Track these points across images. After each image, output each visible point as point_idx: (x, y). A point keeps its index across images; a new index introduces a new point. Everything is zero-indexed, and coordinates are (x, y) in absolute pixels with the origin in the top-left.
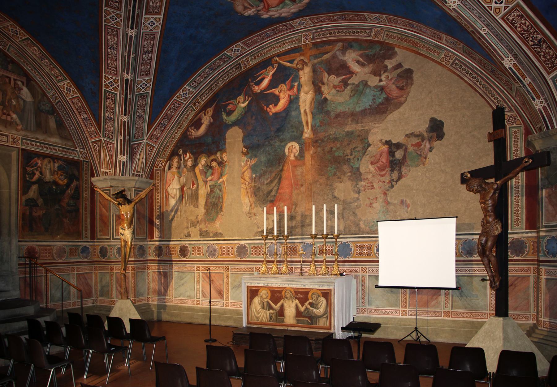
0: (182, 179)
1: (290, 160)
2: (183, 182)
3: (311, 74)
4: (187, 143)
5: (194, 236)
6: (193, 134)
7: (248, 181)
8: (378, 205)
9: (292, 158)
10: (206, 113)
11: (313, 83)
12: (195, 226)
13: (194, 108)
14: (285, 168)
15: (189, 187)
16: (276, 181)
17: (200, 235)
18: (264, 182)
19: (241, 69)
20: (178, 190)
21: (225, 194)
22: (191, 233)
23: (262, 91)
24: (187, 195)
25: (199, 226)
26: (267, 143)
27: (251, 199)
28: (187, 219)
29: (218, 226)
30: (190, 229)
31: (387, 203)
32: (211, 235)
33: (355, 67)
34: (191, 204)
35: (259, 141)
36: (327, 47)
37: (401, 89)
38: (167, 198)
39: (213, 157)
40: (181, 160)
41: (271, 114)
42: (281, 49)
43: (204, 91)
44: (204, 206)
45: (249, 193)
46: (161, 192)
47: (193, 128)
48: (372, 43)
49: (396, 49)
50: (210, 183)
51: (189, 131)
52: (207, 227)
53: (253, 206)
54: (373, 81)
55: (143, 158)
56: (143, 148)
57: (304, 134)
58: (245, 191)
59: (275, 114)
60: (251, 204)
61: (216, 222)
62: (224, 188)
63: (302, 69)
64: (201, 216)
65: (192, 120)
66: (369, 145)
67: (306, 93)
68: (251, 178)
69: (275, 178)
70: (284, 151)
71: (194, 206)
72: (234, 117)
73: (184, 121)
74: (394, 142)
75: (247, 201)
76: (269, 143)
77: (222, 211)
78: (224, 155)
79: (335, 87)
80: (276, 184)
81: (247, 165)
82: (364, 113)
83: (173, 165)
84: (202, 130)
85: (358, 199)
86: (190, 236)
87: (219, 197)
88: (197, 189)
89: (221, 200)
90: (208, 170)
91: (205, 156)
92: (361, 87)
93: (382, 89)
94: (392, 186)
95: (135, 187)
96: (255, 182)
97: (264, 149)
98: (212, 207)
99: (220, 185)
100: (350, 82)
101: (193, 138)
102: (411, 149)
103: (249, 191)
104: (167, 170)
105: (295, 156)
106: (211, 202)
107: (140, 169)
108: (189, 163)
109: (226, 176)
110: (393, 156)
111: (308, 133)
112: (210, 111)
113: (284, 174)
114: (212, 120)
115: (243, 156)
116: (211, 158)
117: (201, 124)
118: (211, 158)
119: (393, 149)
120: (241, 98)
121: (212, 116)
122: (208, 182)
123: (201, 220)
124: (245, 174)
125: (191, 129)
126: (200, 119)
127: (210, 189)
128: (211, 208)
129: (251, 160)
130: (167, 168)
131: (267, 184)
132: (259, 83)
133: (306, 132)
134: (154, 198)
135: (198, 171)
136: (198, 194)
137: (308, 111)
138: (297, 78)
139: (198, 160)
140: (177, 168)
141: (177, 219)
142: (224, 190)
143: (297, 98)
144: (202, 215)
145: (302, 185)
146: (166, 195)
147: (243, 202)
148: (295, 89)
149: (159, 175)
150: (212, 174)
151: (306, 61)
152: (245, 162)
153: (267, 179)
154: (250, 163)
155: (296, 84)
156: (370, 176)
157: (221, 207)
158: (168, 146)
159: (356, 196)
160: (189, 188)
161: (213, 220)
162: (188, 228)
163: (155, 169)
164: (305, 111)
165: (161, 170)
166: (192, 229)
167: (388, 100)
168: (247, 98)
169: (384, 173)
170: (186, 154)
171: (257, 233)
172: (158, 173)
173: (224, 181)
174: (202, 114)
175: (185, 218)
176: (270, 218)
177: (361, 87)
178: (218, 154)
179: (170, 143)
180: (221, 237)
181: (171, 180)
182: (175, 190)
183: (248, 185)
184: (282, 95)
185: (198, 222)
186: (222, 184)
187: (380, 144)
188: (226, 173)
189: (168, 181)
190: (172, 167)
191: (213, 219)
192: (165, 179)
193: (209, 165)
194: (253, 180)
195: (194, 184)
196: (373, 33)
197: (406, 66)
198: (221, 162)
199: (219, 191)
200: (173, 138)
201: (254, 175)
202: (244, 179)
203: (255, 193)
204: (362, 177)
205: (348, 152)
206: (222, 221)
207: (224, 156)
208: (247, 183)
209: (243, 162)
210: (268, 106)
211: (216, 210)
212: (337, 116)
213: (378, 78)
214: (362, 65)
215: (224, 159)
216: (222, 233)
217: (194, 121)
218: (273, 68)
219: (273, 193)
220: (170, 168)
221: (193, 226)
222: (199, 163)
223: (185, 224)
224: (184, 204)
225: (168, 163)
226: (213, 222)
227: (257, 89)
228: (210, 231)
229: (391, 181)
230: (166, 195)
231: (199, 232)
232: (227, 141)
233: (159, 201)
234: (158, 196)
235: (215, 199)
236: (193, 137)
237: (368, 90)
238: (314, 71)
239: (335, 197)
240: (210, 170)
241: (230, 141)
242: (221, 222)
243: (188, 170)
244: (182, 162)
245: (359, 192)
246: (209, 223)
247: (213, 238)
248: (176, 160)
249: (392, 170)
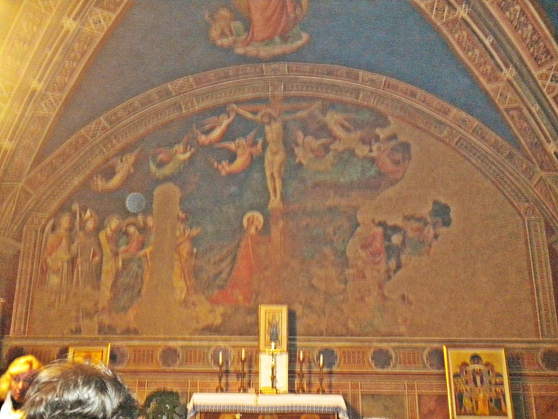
3: (281, 131)
8: (372, 300)
9: (253, 230)
10: (124, 159)
11: (285, 143)
14: (243, 244)
16: (229, 259)
18: (209, 259)
19: (182, 110)
23: (211, 144)
26: (217, 209)
31: (384, 298)
33: (339, 132)
36: (304, 104)
37: (397, 163)
39: (131, 219)
41: (223, 173)
42: (241, 96)
48: (359, 108)
49: (390, 118)
54: (362, 150)
57: (271, 202)
59: (231, 175)
63: (269, 123)
66: (358, 225)
67: (274, 153)
68: (191, 253)
70: (241, 222)
72: (167, 170)
74: (390, 223)
75: (182, 284)
79: (312, 151)
82: (351, 186)
84: (116, 181)
85: (344, 290)
89: (139, 280)
92: (346, 156)
93: (373, 161)
94: (389, 278)
100: (332, 147)
101: (100, 190)
102: (410, 234)
105: (257, 229)
108: (90, 225)
110: (389, 240)
111: (275, 202)
112: (130, 158)
113: (241, 253)
114: (132, 170)
116: (127, 221)
119: (389, 232)
120: (180, 147)
121: (133, 165)
123: (103, 309)
124: (182, 246)
127: (123, 264)
131: (215, 263)
132: (207, 132)
133: (273, 201)
137: (276, 175)
138: (262, 133)
139: (106, 221)
143: (261, 159)
145: (266, 268)
148: (259, 146)
150: (127, 243)
151: (274, 114)
155: (260, 141)
156: (360, 263)
159: (343, 286)
161: (125, 309)
164: (272, 175)
166: (85, 323)
167: (380, 174)
168: (189, 148)
169: (378, 259)
171: (196, 330)
174: (117, 160)
177: (346, 156)
184: (240, 152)
187: (372, 225)
193: (124, 229)
194: (194, 257)
195: (94, 255)
196: (361, 95)
197: (402, 138)
201: (195, 250)
204: (350, 262)
205: (330, 230)
207: (149, 219)
210: (219, 162)
212: (316, 185)
213: (367, 148)
214: (347, 130)
218: (229, 117)
219: (224, 275)
227: (203, 138)
229: (388, 271)
237: (355, 160)
238: (285, 127)
239: (312, 286)
240: (124, 238)
243: (86, 234)
245: (346, 282)
249: (389, 258)
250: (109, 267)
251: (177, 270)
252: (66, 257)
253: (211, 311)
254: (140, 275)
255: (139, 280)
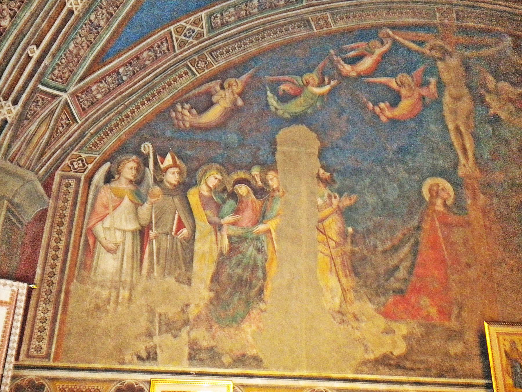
0: (145, 210)
1: (434, 211)
2: (148, 217)
4: (169, 134)
5: (171, 360)
6: (187, 119)
7: (335, 238)
10: (226, 85)
12: (174, 332)
13: (193, 69)
15: (165, 231)
16: (407, 248)
17: (191, 358)
18: (375, 247)
20: (129, 236)
21: (272, 259)
22: (158, 350)
24: (158, 249)
25: (189, 333)
26: (378, 169)
27: (344, 280)
28: (151, 311)
29: (250, 338)
30: (157, 339)
32: (226, 359)
34: (170, 273)
35: (358, 162)
38: (89, 251)
39: (241, 174)
40: (147, 165)
43: (220, 44)
44: (208, 283)
45: (339, 266)
46: (70, 233)
47: (187, 106)
50: (226, 231)
51: (176, 111)
52: (213, 337)
53: (351, 295)
55: (42, 137)
56: (52, 112)
58: (327, 259)
59: (393, 121)
60: (344, 291)
61: (245, 325)
62: (270, 245)
64: (197, 306)
65: (187, 90)
68: (344, 234)
69: (403, 242)
71: (177, 280)
73: (164, 88)
75: (333, 282)
76: (384, 169)
77: (262, 300)
78: (271, 175)
80: (406, 255)
81: (331, 204)
83: (119, 174)
86: (155, 359)
87: (255, 267)
88: (191, 240)
89: (260, 274)
90: (224, 202)
91: (217, 169)
95: (9, 201)
96: (352, 242)
97: (373, 180)
98: (234, 288)
99: (258, 239)
103: (338, 261)
104: (99, 181)
105: (445, 205)
106: (230, 276)
107: (26, 162)
109: (277, 220)
114: (240, 102)
115: (321, 184)
117: (211, 104)
118: (235, 176)
122: (225, 228)
123: (198, 317)
124: (326, 223)
125: (182, 108)
126: (209, 94)
127: (231, 243)
128: (229, 290)
129: (341, 196)
130: (99, 176)
131: (385, 252)
134: (44, 243)
135: (197, 198)
136: (192, 251)
139: (199, 174)
140: (131, 181)
141: (115, 310)
142: (268, 249)
144: (202, 304)
146: (87, 242)
147: (321, 284)
149: (72, 190)
150: (237, 211)
152: (326, 197)
153: (383, 242)
154: (340, 202)
157: (261, 291)
158: (111, 130)
160: (167, 234)
162: (150, 335)
163: (58, 173)
165: (78, 180)
170: (164, 156)
172: (69, 185)
173: (269, 231)
174: (215, 85)
175: (145, 309)
176: (396, 330)
178: (255, 171)
179: (117, 125)
180: (258, 367)
181: (111, 208)
182: (119, 234)
183: (336, 247)
185: (186, 322)
186: (263, 237)
188: (274, 213)
189: (99, 208)
190: (117, 176)
191: (234, 319)
192: (90, 201)
193: (229, 189)
194: (349, 240)
195: (180, 226)
198: (262, 189)
199: (255, 252)
200: (128, 116)
201: (350, 230)
202: (324, 233)
203: (353, 267)
206: (261, 325)
208: (332, 244)
209: (322, 197)
211: (244, 296)
215: (271, 183)
216: (261, 356)
217: (190, 94)
220: (109, 178)
221: (167, 332)
222: (201, 181)
223: (143, 322)
224: (144, 272)
225: (106, 167)
226: (235, 325)
228: (222, 349)
230: (87, 242)
231: (187, 348)
232: (279, 148)
233: (60, 254)
234: (58, 240)
235: (244, 270)
236: (188, 124)
240: (231, 202)
241: (285, 148)
242: (258, 327)
243: (167, 192)
244: (150, 171)
246: (222, 328)
247: (232, 368)
248: (133, 165)
250: (207, 247)
251: (323, 260)
252: (133, 226)
253: (387, 331)
254: (259, 263)
255: (260, 274)
